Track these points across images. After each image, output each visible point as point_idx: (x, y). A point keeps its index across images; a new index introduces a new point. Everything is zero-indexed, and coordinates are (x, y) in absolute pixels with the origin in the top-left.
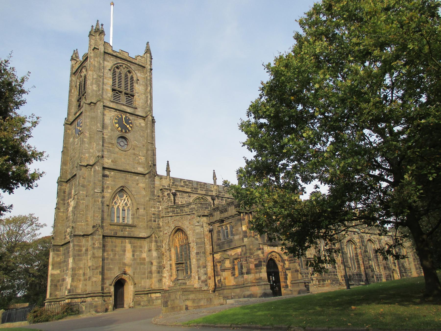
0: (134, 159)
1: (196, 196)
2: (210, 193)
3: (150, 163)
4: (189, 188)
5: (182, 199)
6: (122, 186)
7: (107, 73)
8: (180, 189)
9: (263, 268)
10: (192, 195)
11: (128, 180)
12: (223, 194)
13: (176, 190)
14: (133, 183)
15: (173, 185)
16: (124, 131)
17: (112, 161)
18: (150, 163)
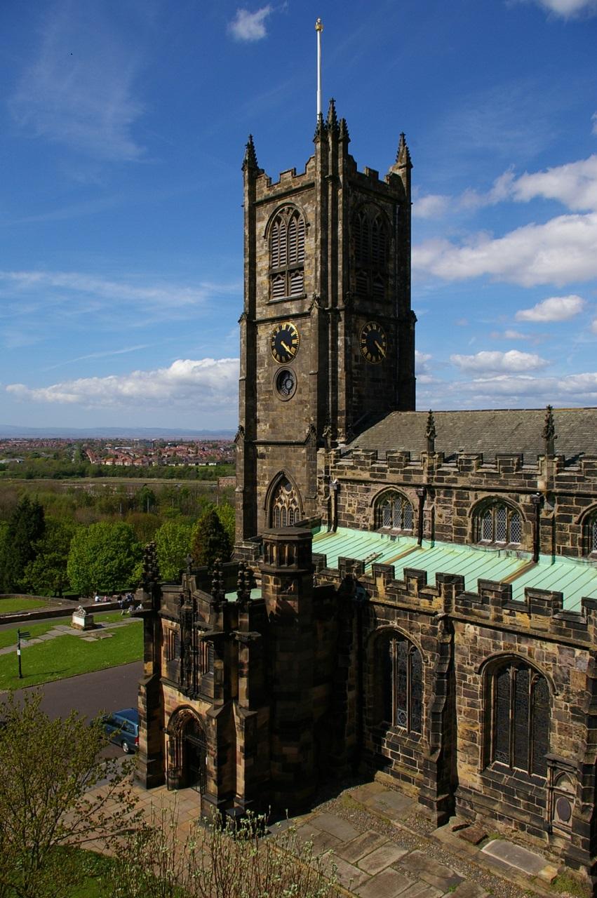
0: (300, 413)
1: (380, 487)
2: (415, 479)
3: (312, 419)
4: (366, 469)
5: (351, 498)
6: (279, 474)
7: (262, 246)
8: (349, 475)
9: (143, 731)
10: (373, 487)
11: (291, 459)
12: (452, 476)
13: (339, 479)
14: (297, 463)
15: (335, 467)
16: (283, 358)
17: (270, 427)
18: (312, 419)
